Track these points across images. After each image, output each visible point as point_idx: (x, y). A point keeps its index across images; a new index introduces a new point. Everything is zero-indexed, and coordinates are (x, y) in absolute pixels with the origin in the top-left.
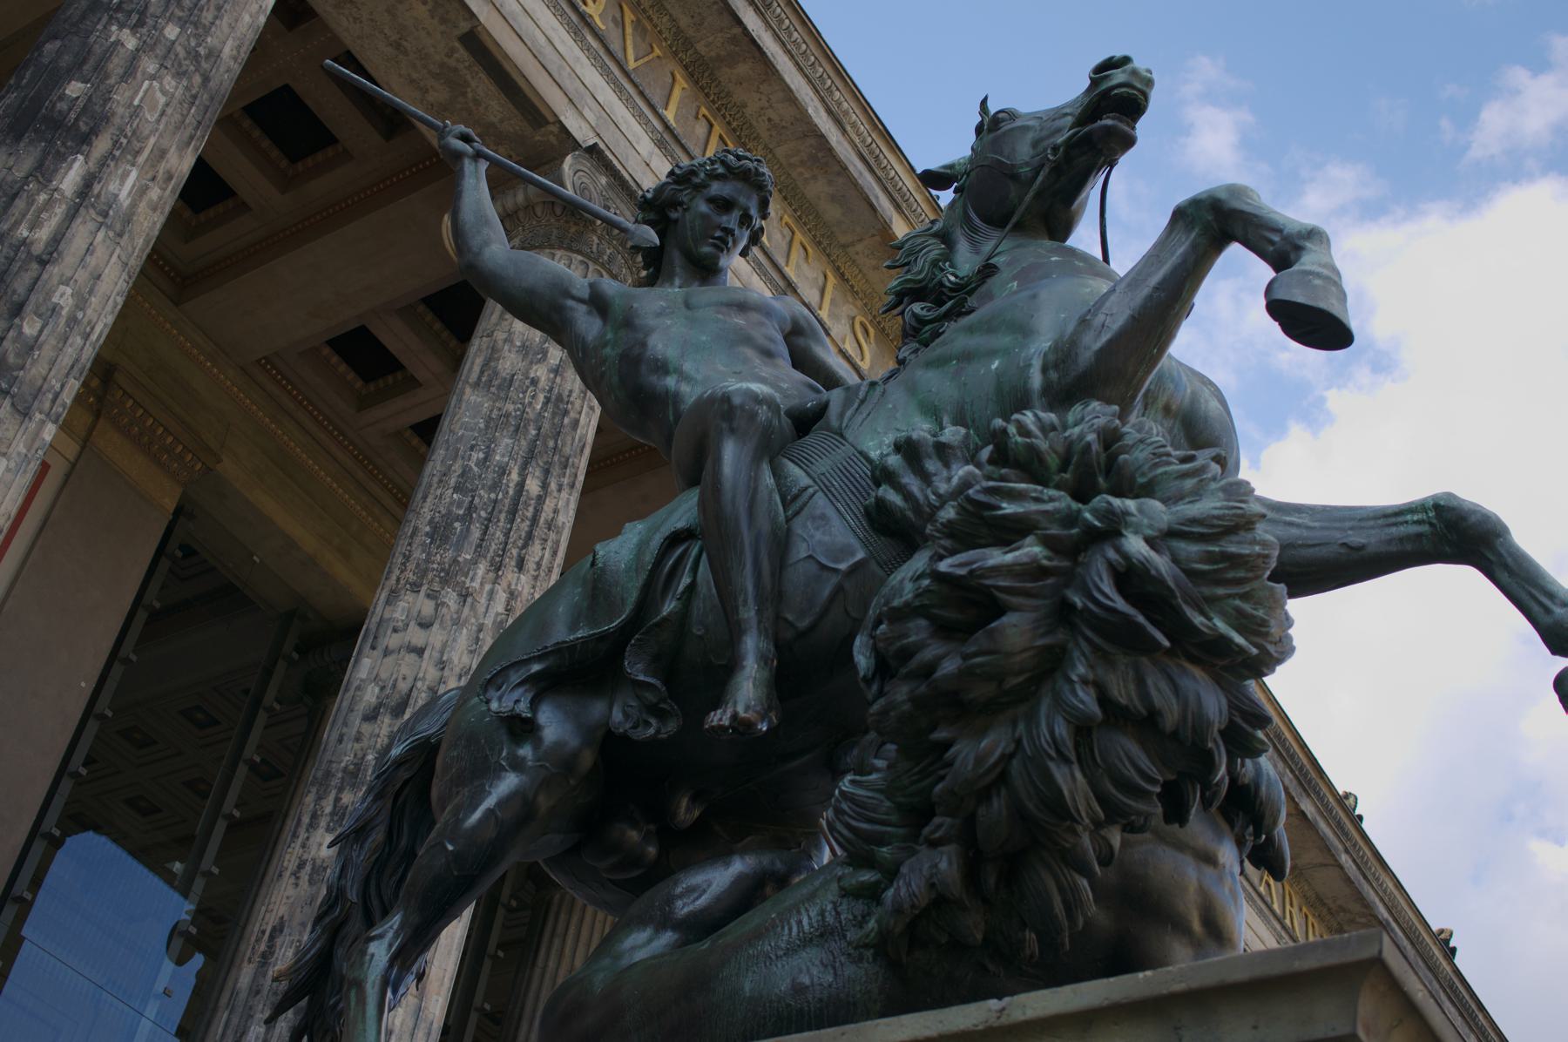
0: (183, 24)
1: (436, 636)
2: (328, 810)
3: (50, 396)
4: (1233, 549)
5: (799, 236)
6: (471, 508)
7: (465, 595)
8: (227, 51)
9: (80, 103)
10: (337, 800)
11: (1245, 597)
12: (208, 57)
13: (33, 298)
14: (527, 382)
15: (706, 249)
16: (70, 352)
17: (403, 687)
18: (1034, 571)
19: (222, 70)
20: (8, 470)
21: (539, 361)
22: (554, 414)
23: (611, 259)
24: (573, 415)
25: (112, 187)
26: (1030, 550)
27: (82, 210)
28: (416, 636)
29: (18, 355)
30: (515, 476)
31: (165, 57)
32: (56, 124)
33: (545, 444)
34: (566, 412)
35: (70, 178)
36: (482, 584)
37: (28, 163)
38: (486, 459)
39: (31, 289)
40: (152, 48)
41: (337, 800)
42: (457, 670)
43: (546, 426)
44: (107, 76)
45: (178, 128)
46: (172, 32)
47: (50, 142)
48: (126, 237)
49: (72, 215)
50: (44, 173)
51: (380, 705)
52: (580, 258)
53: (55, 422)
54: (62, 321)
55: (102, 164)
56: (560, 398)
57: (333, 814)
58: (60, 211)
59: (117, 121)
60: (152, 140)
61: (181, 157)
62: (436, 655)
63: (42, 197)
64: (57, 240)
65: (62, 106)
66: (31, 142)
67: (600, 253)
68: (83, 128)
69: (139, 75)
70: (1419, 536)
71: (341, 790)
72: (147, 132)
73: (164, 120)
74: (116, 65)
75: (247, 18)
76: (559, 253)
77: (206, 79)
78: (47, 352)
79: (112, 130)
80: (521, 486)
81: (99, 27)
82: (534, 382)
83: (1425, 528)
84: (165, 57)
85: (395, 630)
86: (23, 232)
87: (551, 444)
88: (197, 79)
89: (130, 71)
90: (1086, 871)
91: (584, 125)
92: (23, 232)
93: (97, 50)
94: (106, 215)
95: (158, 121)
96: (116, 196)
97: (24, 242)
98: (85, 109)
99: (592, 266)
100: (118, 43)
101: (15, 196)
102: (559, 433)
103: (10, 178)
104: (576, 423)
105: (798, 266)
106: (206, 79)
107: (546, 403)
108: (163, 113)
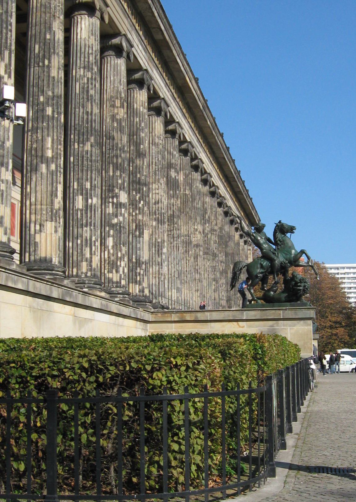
1: (160, 190)
6: (158, 169)
7: (161, 184)
17: (157, 199)
28: (157, 191)
32: (142, 154)
38: (158, 159)
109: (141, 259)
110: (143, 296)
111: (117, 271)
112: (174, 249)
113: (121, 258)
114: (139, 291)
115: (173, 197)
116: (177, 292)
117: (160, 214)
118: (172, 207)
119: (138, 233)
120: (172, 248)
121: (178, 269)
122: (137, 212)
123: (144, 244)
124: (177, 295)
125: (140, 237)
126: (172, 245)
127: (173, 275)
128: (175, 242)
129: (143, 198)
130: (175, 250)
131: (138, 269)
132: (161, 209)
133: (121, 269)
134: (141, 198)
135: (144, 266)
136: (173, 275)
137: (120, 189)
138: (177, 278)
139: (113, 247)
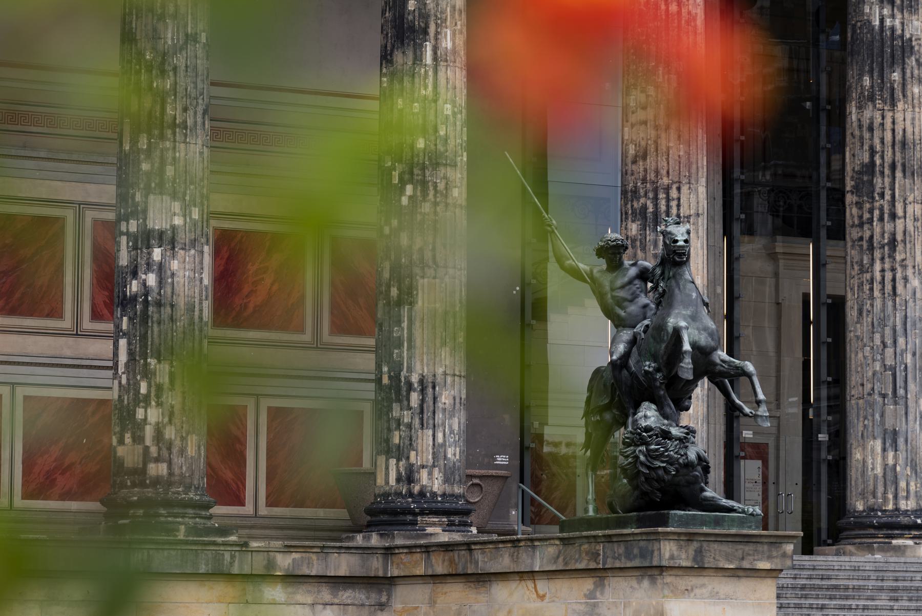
2: (630, 212)
10: (632, 206)
17: (643, 143)
18: (630, 463)
25: (444, 45)
30: (663, 7)
32: (412, 29)
36: (663, 77)
41: (632, 206)
42: (664, 127)
51: (636, 156)
55: (436, 39)
57: (632, 213)
58: (431, 73)
59: (432, 12)
62: (652, 123)
63: (423, 70)
65: (410, 17)
66: (408, 45)
68: (422, 25)
71: (632, 201)
79: (433, 18)
80: (667, 10)
85: (633, 113)
109: (404, 373)
110: (411, 494)
111: (138, 439)
112: (872, 289)
113: (147, 397)
114: (399, 480)
115: (872, 98)
116: (884, 450)
117: (651, 195)
118: (867, 135)
119: (394, 292)
120: (867, 287)
121: (889, 362)
122: (395, 223)
123: (417, 324)
124: (884, 458)
125: (399, 303)
126: (868, 276)
127: (868, 386)
128: (878, 266)
130: (877, 293)
132: (657, 172)
133: (149, 431)
134: (407, 177)
135: (415, 397)
136: (868, 386)
137: (148, 191)
138: (884, 396)
139: (127, 365)
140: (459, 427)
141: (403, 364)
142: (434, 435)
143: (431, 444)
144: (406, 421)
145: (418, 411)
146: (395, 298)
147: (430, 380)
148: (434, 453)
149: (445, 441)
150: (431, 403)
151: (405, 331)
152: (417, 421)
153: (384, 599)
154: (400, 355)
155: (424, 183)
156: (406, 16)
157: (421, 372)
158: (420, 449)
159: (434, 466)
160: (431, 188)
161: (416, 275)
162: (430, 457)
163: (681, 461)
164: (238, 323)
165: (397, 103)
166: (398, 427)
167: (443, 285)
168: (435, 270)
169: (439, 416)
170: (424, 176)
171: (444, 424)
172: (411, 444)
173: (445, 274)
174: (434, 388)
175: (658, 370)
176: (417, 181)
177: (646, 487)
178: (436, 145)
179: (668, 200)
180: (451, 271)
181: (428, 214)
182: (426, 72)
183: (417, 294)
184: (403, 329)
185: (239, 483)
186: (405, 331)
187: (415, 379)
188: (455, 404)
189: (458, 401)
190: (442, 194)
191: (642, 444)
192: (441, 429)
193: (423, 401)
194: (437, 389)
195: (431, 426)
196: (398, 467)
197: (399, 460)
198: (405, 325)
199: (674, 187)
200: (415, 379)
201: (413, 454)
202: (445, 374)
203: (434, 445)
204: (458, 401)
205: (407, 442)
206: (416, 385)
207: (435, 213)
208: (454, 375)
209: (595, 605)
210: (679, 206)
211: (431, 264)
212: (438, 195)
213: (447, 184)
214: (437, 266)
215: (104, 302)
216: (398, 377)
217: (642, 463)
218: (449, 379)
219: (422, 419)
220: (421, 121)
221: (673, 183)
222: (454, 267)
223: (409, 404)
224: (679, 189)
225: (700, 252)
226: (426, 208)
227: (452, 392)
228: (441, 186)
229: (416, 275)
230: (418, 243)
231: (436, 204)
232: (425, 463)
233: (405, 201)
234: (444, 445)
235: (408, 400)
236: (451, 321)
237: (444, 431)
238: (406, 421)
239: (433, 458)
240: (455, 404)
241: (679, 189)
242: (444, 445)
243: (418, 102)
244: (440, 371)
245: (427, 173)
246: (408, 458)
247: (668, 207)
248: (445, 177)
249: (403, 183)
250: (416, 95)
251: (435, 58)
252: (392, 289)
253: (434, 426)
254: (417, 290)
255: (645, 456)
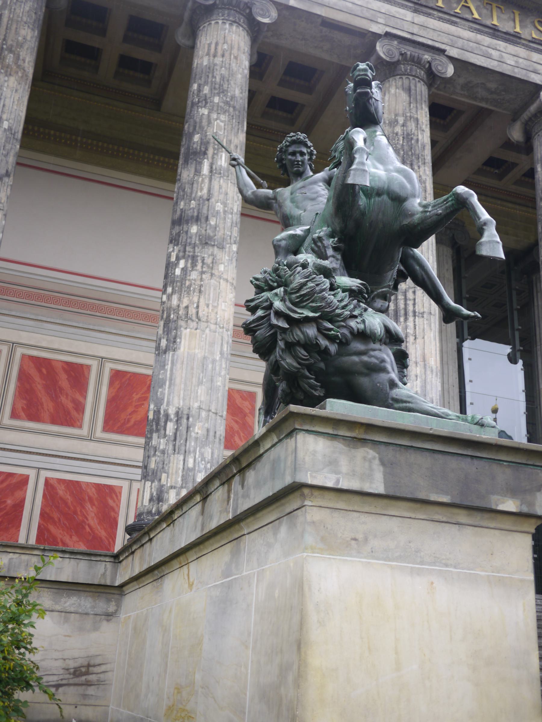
0: (218, 94)
3: (229, 238)
4: (302, 293)
5: (494, 5)
8: (237, 92)
9: (199, 142)
11: (312, 302)
12: (231, 100)
13: (210, 213)
14: (395, 135)
15: (295, 169)
16: (229, 221)
18: (261, 318)
19: (239, 99)
20: (225, 266)
21: (396, 125)
22: (408, 142)
23: (411, 70)
24: (415, 138)
25: (219, 163)
26: (260, 313)
27: (213, 177)
29: (213, 232)
31: (218, 110)
32: (195, 153)
33: (408, 155)
34: (412, 139)
35: (206, 169)
37: (193, 170)
39: (208, 211)
40: (212, 109)
43: (406, 148)
44: (203, 128)
45: (232, 130)
46: (216, 100)
47: (196, 160)
48: (230, 176)
49: (210, 180)
50: (198, 172)
52: (399, 77)
53: (235, 243)
54: (222, 214)
55: (213, 158)
56: (408, 135)
58: (207, 181)
60: (225, 140)
61: (237, 138)
63: (200, 179)
64: (209, 190)
65: (195, 146)
66: (191, 163)
67: (406, 70)
68: (203, 149)
69: (212, 121)
70: (453, 204)
72: (222, 138)
73: (226, 131)
74: (205, 122)
75: (240, 76)
76: (391, 79)
77: (234, 107)
78: (221, 226)
79: (212, 145)
81: (196, 112)
82: (397, 134)
83: (453, 202)
84: (218, 110)
86: (199, 194)
87: (410, 153)
88: (231, 109)
89: (209, 122)
90: (311, 378)
91: (380, 26)
92: (199, 194)
93: (198, 120)
94: (220, 173)
95: (224, 133)
96: (221, 165)
97: (200, 197)
98: (201, 143)
99: (404, 77)
100: (203, 114)
101: (193, 183)
102: (411, 148)
103: (190, 179)
104: (417, 140)
105: (498, 18)
106: (234, 107)
107: (403, 140)
108: (225, 129)
114: (151, 500)
123: (178, 366)
129: (185, 251)
131: (155, 435)
140: (212, 456)
141: (163, 399)
142: (184, 460)
143: (181, 467)
144: (162, 447)
145: (172, 438)
146: (164, 348)
147: (185, 412)
148: (183, 476)
149: (194, 466)
150: (184, 432)
151: (168, 373)
152: (171, 447)
153: (112, 608)
154: (163, 394)
155: (194, 258)
156: (192, 145)
157: (177, 405)
158: (170, 471)
159: (182, 487)
160: (200, 261)
161: (181, 326)
162: (180, 479)
163: (353, 323)
164: (122, 431)
165: (180, 205)
166: (155, 455)
167: (204, 336)
168: (197, 323)
169: (192, 444)
170: (194, 252)
171: (195, 452)
172: (163, 468)
173: (207, 327)
174: (188, 419)
175: (331, 235)
176: (189, 256)
177: (289, 362)
178: (206, 230)
179: (406, 299)
180: (213, 327)
181: (195, 280)
182: (203, 180)
183: (180, 342)
184: (166, 370)
185: (111, 540)
186: (168, 373)
187: (172, 411)
188: (208, 435)
189: (211, 434)
190: (208, 266)
191: (279, 286)
192: (192, 455)
193: (177, 430)
194: (191, 419)
195: (183, 451)
196: (151, 489)
197: (152, 482)
198: (168, 367)
199: (411, 291)
200: (172, 411)
201: (164, 476)
202: (200, 408)
203: (184, 468)
204: (211, 434)
205: (161, 466)
206: (172, 416)
207: (201, 280)
208: (209, 411)
209: (229, 586)
210: (414, 304)
211: (194, 318)
212: (204, 266)
213: (213, 259)
214: (199, 320)
215: (23, 408)
216: (159, 412)
217: (279, 314)
218: (203, 414)
219: (174, 446)
220: (196, 214)
221: (409, 288)
222: (216, 324)
223: (165, 433)
224: (414, 292)
225: (433, 343)
226: (194, 275)
227: (206, 425)
228: (209, 261)
229: (181, 326)
230: (185, 302)
231: (202, 273)
232: (173, 484)
233: (178, 272)
234: (193, 469)
235: (165, 429)
236: (210, 366)
237: (195, 457)
238: (162, 447)
239: (182, 480)
240: (208, 435)
241: (414, 292)
242: (193, 469)
243: (195, 200)
244: (196, 405)
245: (197, 250)
246: (160, 480)
247: (406, 304)
248: (212, 255)
249: (178, 259)
250: (193, 195)
251: (211, 171)
252: (162, 340)
253: (185, 452)
254: (180, 338)
255: (283, 300)
